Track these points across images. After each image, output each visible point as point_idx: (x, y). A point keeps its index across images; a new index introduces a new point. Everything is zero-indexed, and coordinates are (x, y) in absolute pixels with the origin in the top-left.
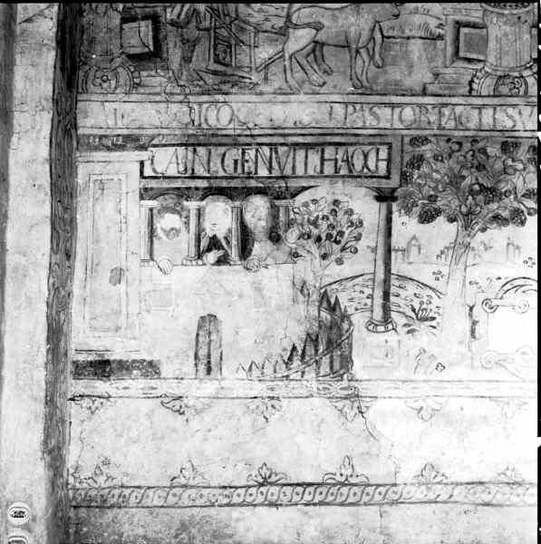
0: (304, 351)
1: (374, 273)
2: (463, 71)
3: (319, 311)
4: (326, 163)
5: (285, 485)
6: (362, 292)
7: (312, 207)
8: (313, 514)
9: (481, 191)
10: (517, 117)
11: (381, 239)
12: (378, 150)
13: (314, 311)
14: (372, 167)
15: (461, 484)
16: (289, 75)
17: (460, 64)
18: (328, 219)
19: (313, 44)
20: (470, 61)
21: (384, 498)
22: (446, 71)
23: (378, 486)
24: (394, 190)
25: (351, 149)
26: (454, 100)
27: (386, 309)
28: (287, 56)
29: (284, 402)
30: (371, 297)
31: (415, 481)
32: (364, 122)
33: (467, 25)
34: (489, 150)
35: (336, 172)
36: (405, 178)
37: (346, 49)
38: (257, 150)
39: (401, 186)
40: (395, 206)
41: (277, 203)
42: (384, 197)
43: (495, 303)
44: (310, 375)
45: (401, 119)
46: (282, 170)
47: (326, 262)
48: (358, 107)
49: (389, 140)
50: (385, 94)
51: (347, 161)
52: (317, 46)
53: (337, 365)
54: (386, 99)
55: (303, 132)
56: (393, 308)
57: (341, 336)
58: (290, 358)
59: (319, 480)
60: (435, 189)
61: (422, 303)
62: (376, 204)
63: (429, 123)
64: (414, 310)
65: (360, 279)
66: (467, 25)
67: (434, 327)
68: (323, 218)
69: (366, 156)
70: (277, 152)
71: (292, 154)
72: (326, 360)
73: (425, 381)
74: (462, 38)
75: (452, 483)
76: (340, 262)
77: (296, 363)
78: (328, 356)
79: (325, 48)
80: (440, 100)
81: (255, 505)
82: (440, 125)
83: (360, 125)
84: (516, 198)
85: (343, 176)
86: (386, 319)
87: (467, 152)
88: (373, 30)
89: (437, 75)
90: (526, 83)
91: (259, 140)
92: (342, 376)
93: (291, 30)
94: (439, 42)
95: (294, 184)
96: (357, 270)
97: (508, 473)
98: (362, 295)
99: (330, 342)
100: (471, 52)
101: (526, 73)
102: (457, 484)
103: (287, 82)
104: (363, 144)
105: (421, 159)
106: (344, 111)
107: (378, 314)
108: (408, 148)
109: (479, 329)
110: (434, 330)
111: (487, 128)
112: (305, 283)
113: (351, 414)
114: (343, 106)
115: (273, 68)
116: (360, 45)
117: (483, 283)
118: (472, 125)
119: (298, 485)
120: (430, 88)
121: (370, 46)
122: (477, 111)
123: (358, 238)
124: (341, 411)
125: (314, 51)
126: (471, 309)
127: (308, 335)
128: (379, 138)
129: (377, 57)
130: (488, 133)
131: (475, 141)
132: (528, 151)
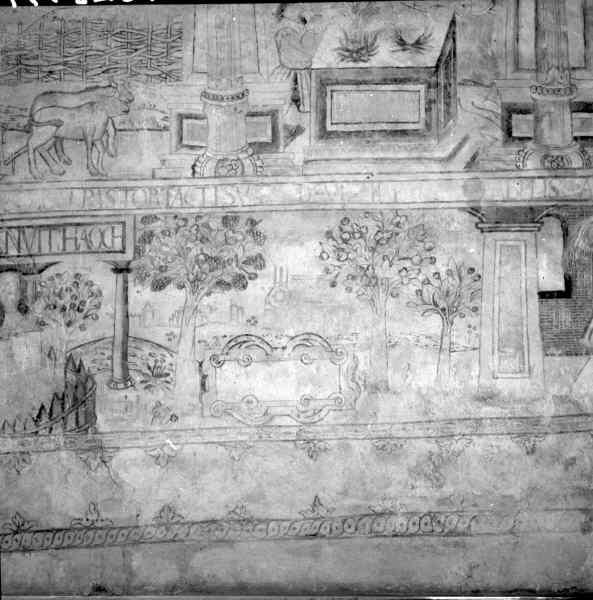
0: (51, 410)
1: (114, 337)
2: (186, 159)
3: (65, 372)
4: (67, 241)
5: (38, 531)
6: (103, 354)
7: (57, 280)
8: (61, 556)
9: (206, 260)
10: (234, 193)
11: (119, 307)
12: (113, 229)
13: (60, 372)
14: (109, 244)
15: (197, 523)
16: (33, 165)
17: (184, 150)
18: (71, 290)
19: (53, 139)
20: (192, 147)
21: (127, 539)
22: (174, 157)
23: (122, 528)
24: (129, 263)
25: (89, 229)
26: (180, 182)
27: (125, 368)
28: (31, 151)
29: (34, 457)
30: (111, 358)
31: (154, 522)
32: (101, 205)
33: (189, 117)
34: (211, 224)
35: (77, 249)
36: (138, 252)
37: (84, 143)
38: (7, 234)
39: (134, 258)
40: (131, 277)
41: (26, 278)
42: (121, 270)
43: (221, 358)
44: (58, 430)
45: (133, 201)
46: (29, 250)
47: (71, 329)
48: (96, 191)
49: (123, 219)
50: (120, 180)
51: (85, 239)
52: (58, 141)
53: (82, 420)
54: (119, 184)
55: (48, 215)
56: (131, 367)
57: (85, 394)
58: (39, 416)
59: (68, 526)
60: (165, 260)
61: (156, 361)
62: (115, 275)
63: (158, 202)
64: (149, 368)
65: (101, 342)
66: (189, 117)
67: (167, 382)
68: (67, 290)
69: (102, 235)
70: (24, 233)
71: (37, 235)
72: (71, 418)
73: (161, 431)
74: (185, 126)
75: (188, 523)
76: (82, 328)
77: (45, 418)
78: (74, 413)
79: (67, 145)
80: (168, 182)
81: (11, 552)
82: (168, 204)
83: (98, 206)
84: (237, 266)
85: (83, 253)
86: (126, 378)
87: (192, 227)
88: (106, 124)
89: (163, 161)
90: (243, 165)
91: (9, 224)
92: (86, 430)
93: (34, 128)
94: (164, 133)
95: (41, 261)
96: (99, 333)
97: (238, 511)
98: (102, 357)
99: (75, 399)
100: (196, 140)
101: (241, 156)
102: (193, 523)
103: (31, 172)
104: (101, 224)
105: (151, 234)
106: (82, 195)
107: (118, 372)
108: (140, 226)
109: (209, 382)
110: (168, 385)
111: (210, 205)
112: (52, 348)
113: (94, 464)
114: (82, 191)
115: (19, 161)
116: (95, 138)
117: (211, 341)
118: (196, 204)
119: (48, 531)
120: (159, 174)
121: (104, 139)
122: (201, 191)
123: (98, 307)
124: (85, 461)
125: (55, 145)
126: (201, 364)
127: (56, 395)
128: (117, 220)
129: (111, 147)
130: (210, 210)
131: (199, 217)
132: (246, 224)
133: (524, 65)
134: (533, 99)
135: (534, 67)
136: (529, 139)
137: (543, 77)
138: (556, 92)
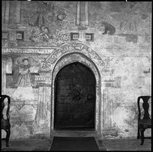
133: (6, 22)
134: (8, 30)
135: (8, 22)
136: (6, 39)
137: (10, 25)
138: (13, 28)
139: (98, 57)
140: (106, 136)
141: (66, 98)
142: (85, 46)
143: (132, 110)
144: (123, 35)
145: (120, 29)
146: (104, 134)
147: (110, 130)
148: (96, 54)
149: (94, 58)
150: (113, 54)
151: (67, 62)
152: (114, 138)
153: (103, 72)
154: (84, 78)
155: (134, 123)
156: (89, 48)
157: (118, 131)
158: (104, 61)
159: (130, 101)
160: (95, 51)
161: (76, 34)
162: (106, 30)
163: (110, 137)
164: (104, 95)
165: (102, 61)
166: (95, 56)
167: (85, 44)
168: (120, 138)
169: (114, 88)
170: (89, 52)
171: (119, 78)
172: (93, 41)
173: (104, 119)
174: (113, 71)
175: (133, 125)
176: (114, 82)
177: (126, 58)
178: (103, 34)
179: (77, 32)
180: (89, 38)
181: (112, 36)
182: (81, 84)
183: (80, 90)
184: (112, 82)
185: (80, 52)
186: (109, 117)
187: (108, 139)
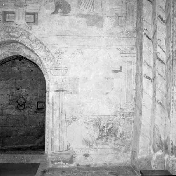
139: (44, 48)
140: (56, 163)
141: (6, 107)
142: (25, 32)
143: (94, 125)
144: (82, 16)
145: (78, 6)
146: (53, 160)
147: (61, 154)
148: (41, 44)
149: (38, 49)
150: (67, 44)
151: (2, 56)
152: (67, 166)
153: (51, 71)
154: (32, 80)
155: (97, 144)
156: (31, 34)
157: (74, 156)
158: (53, 54)
159: (92, 113)
160: (40, 39)
161: (10, 14)
162: (57, 7)
163: (63, 165)
164: (53, 104)
165: (51, 54)
166: (40, 46)
167: (24, 28)
168: (76, 165)
169: (68, 94)
170: (30, 41)
171: (76, 79)
172: (37, 24)
173: (53, 138)
174: (68, 69)
175: (96, 147)
176: (68, 85)
177: (87, 49)
178: (52, 13)
179: (14, 10)
180: (31, 20)
181: (66, 18)
182: (28, 88)
183: (26, 96)
184: (65, 86)
185: (17, 40)
186: (61, 135)
187: (58, 167)
